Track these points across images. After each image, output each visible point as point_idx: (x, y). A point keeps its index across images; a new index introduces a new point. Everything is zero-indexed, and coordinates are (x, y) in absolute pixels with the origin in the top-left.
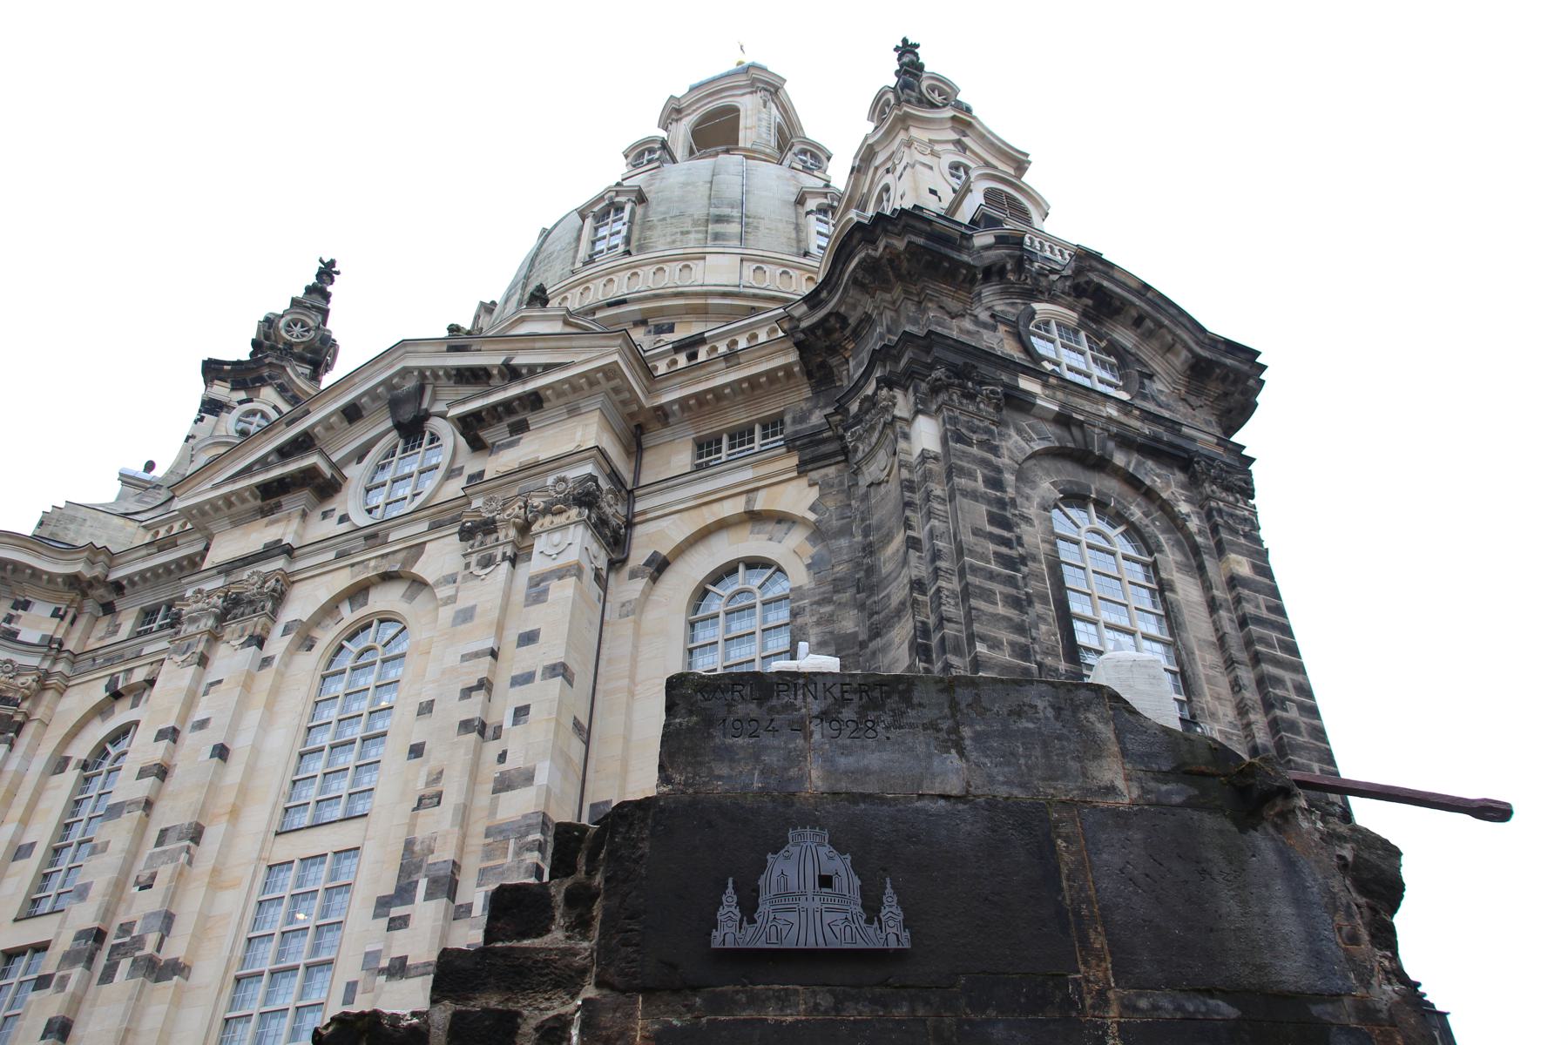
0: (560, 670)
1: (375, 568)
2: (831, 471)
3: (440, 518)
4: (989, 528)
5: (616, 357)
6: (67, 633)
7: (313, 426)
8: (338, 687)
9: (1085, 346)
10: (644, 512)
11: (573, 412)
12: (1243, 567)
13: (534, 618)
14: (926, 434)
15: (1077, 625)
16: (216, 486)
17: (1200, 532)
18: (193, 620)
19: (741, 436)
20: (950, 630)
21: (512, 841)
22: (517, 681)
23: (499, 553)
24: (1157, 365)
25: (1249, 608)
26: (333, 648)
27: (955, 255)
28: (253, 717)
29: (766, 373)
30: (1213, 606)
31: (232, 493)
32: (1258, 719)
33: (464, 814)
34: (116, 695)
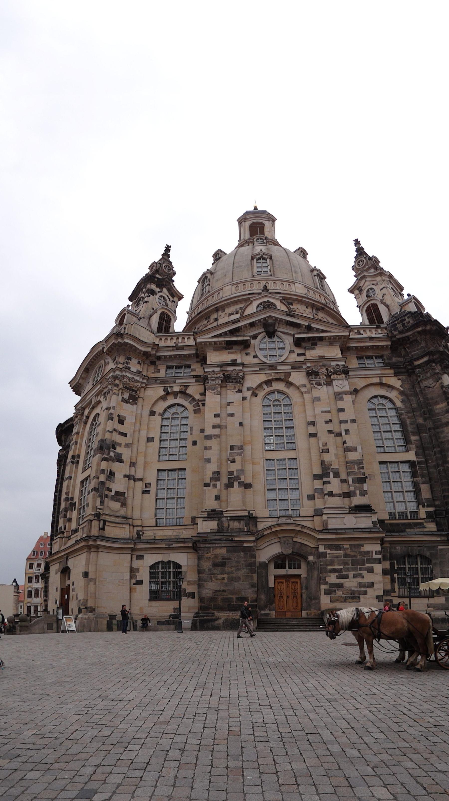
1: (274, 376)
3: (296, 366)
7: (241, 326)
11: (331, 344)
13: (341, 404)
18: (213, 380)
22: (341, 422)
23: (322, 382)
28: (247, 415)
31: (218, 341)
33: (336, 455)
34: (168, 394)
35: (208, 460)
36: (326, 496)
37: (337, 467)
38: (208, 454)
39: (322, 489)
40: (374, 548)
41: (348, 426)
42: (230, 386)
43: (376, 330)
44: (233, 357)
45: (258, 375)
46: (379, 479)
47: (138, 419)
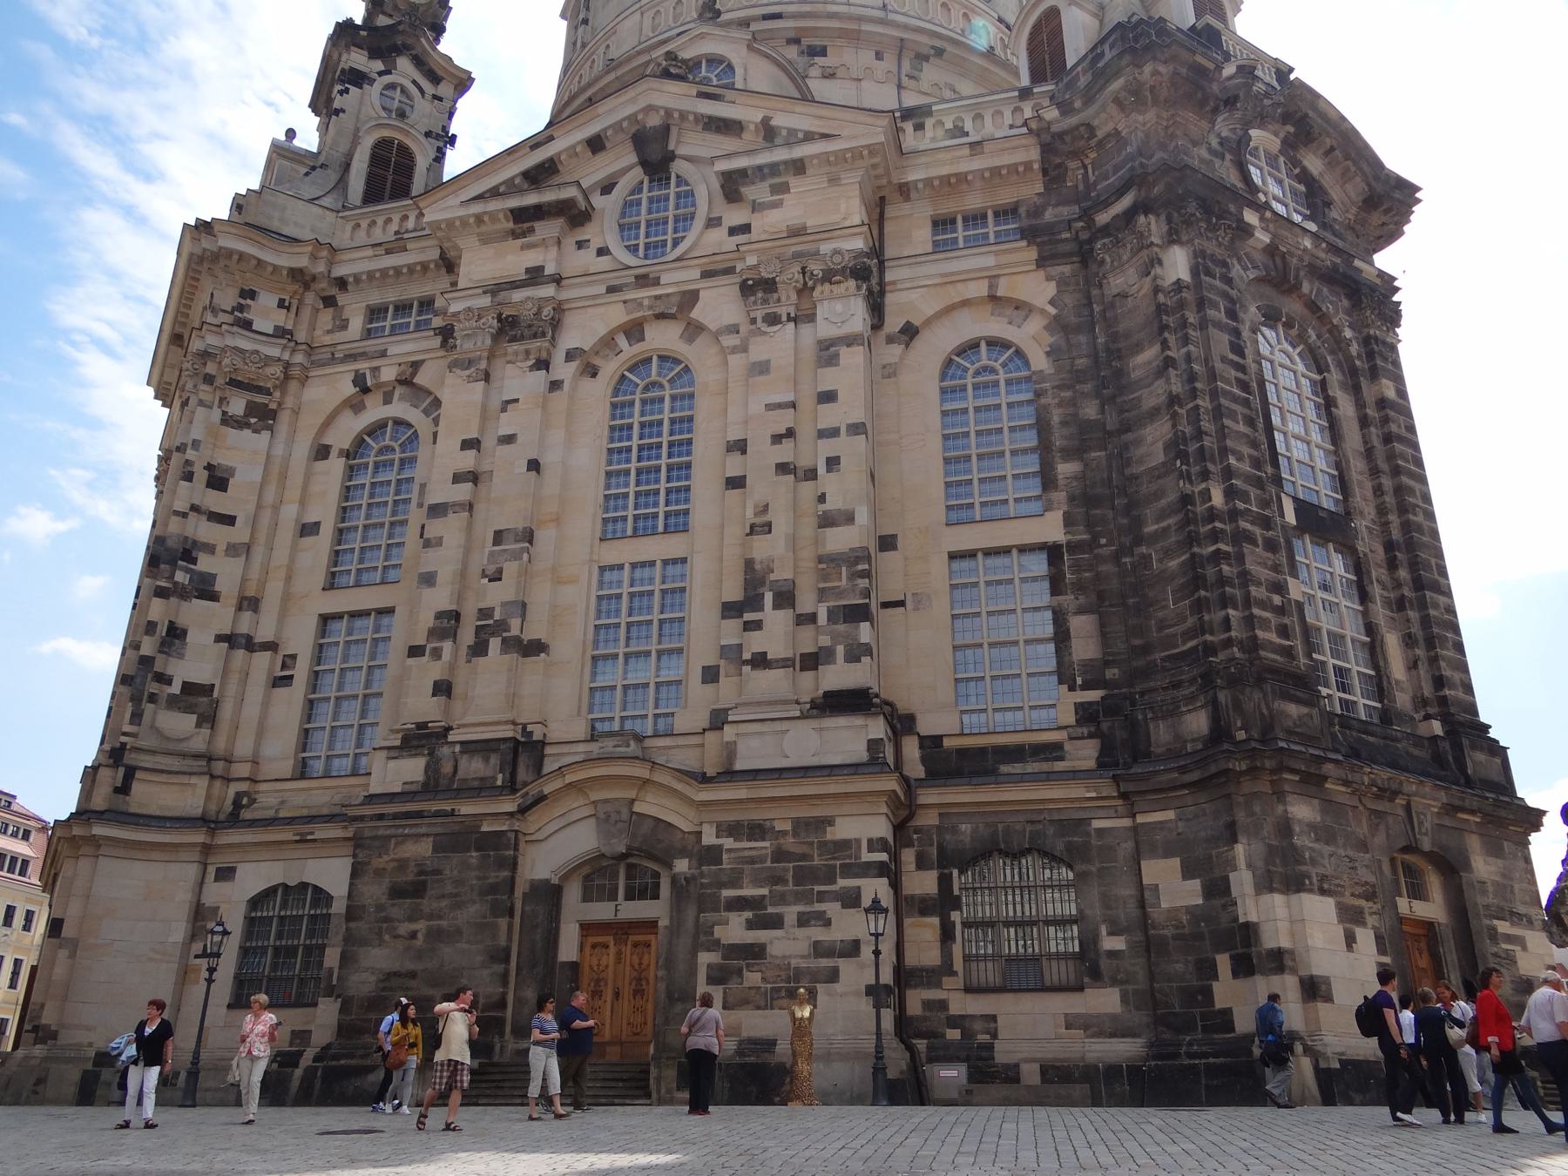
0: (857, 429)
1: (650, 308)
7: (559, 154)
10: (893, 283)
11: (834, 181)
12: (1391, 394)
13: (828, 379)
14: (1177, 264)
17: (1359, 356)
20: (1207, 442)
22: (822, 434)
23: (783, 311)
24: (1335, 193)
25: (1394, 428)
26: (617, 377)
28: (557, 436)
29: (1008, 166)
30: (1364, 422)
32: (1393, 517)
33: (793, 541)
34: (366, 390)
35: (428, 579)
36: (747, 669)
37: (788, 575)
38: (430, 560)
39: (740, 646)
40: (864, 826)
41: (845, 446)
43: (1017, 110)
45: (601, 310)
46: (941, 607)
47: (275, 470)
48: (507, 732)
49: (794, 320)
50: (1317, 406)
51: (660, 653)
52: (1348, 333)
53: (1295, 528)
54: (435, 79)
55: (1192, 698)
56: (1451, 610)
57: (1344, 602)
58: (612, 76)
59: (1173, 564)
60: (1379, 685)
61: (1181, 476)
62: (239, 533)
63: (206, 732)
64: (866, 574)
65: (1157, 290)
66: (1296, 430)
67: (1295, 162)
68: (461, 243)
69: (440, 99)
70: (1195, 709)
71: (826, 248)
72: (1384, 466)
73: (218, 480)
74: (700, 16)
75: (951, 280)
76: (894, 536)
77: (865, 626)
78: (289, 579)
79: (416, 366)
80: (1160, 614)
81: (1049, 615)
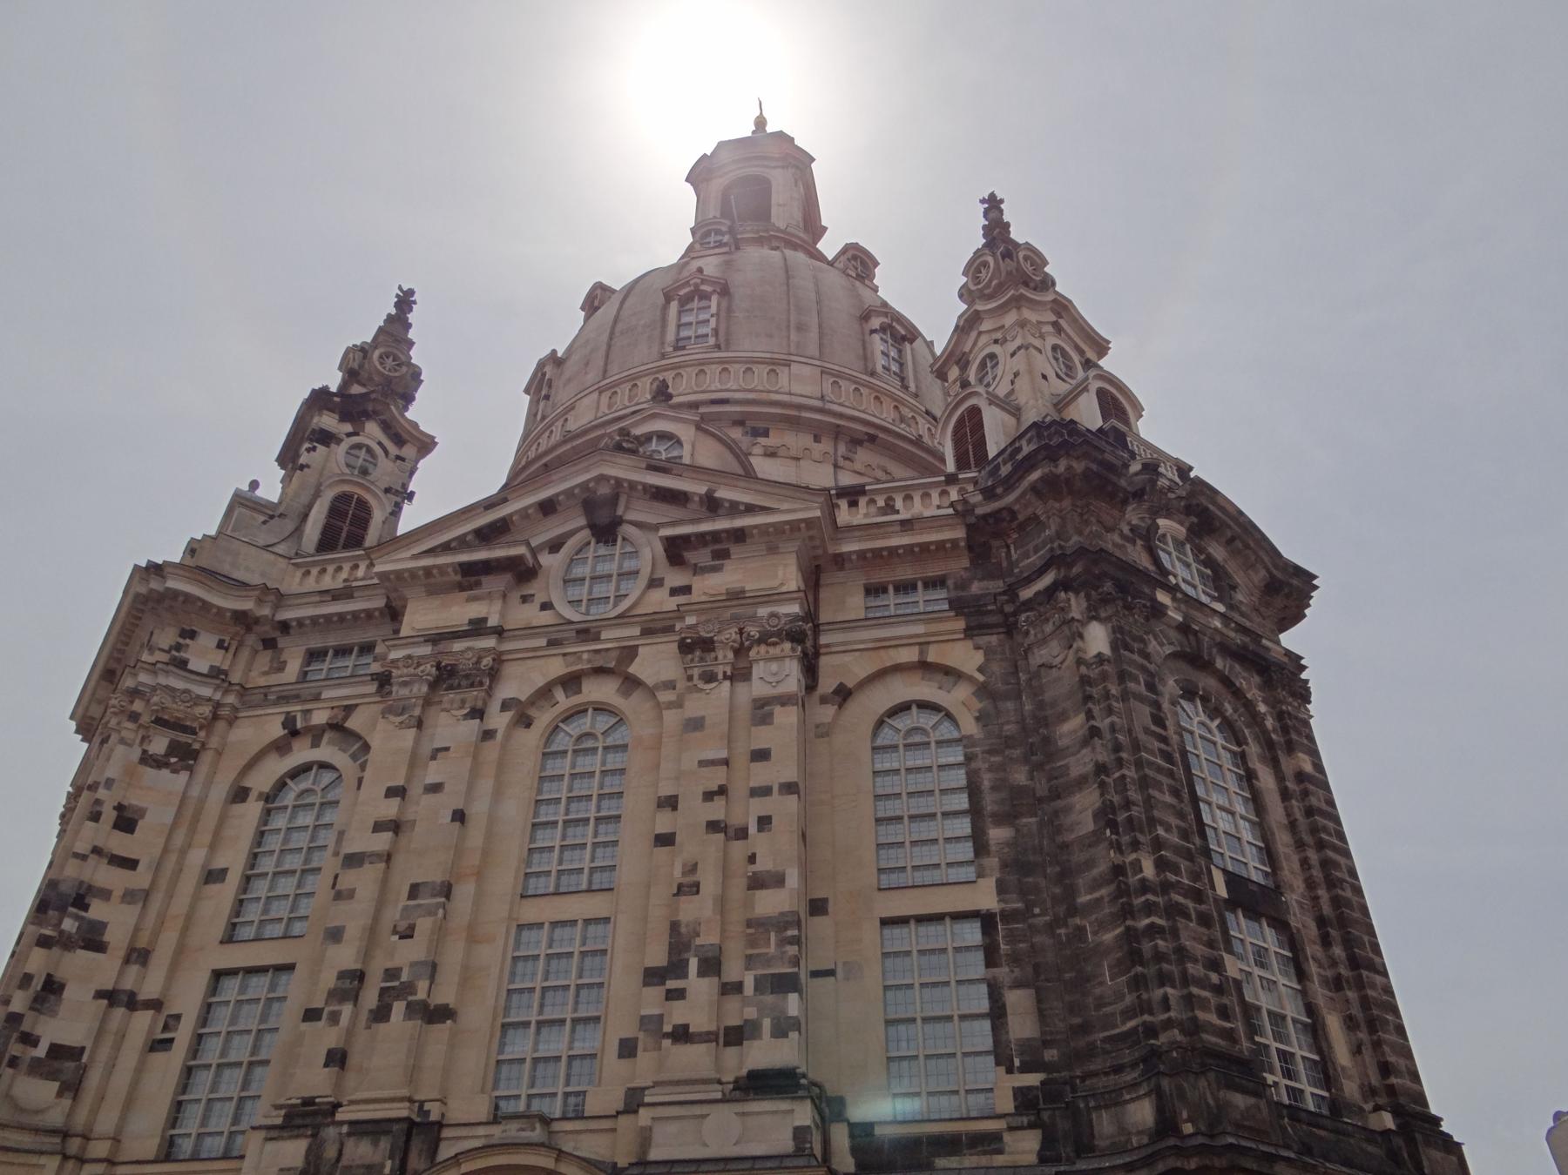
0: (790, 788)
1: (589, 661)
2: (994, 639)
3: (654, 627)
4: (1153, 728)
5: (818, 513)
6: (231, 665)
7: (511, 515)
8: (564, 766)
9: (1190, 559)
10: (827, 646)
11: (773, 550)
13: (762, 737)
14: (1097, 639)
15: (1202, 805)
16: (415, 557)
17: (1274, 730)
18: (405, 684)
19: (905, 587)
21: (773, 935)
23: (720, 670)
24: (1239, 578)
25: (1314, 801)
27: (1114, 478)
28: (486, 785)
30: (1285, 795)
32: (1322, 892)
33: (722, 903)
34: (294, 733)
35: (335, 935)
36: (667, 1043)
39: (661, 1016)
42: (452, 696)
43: (944, 493)
44: (476, 610)
47: (189, 812)
48: (401, 1111)
49: (731, 678)
50: (1240, 777)
51: (575, 1021)
52: (1262, 708)
53: (1225, 901)
54: (399, 441)
55: (1134, 1085)
56: (1389, 991)
57: (1282, 980)
58: (568, 446)
59: (1108, 937)
60: (1325, 1072)
61: (1111, 845)
62: (139, 879)
63: (66, 1102)
64: (796, 941)
65: (1080, 662)
66: (1221, 802)
67: (1198, 550)
68: (407, 593)
69: (403, 459)
70: (1138, 1098)
71: (763, 612)
72: (1307, 838)
73: (126, 821)
74: (654, 398)
75: (882, 646)
76: (825, 901)
77: (793, 998)
78: (185, 930)
79: (349, 710)
80: (1098, 991)
81: (984, 988)
